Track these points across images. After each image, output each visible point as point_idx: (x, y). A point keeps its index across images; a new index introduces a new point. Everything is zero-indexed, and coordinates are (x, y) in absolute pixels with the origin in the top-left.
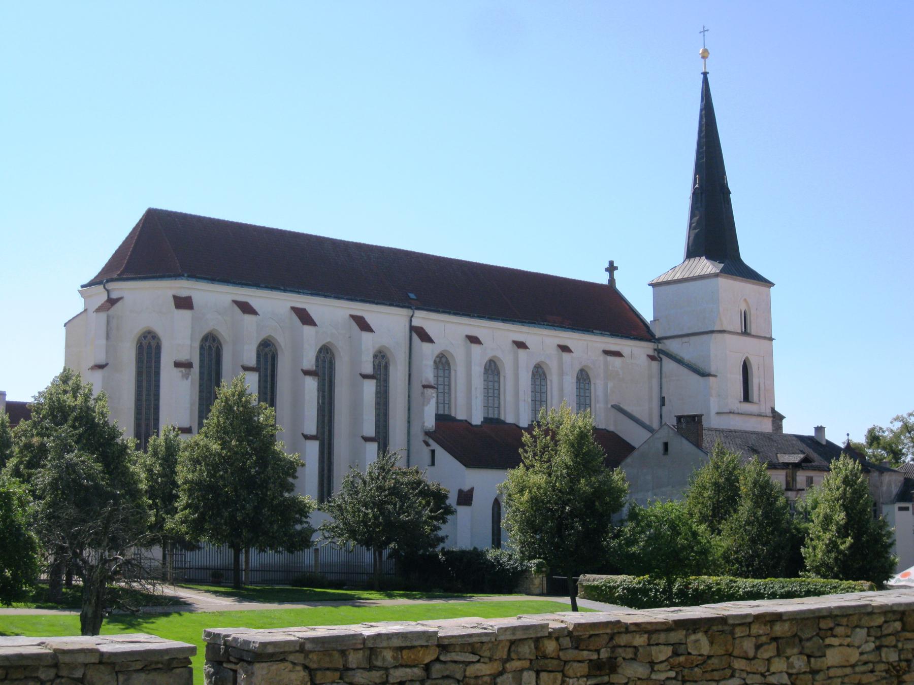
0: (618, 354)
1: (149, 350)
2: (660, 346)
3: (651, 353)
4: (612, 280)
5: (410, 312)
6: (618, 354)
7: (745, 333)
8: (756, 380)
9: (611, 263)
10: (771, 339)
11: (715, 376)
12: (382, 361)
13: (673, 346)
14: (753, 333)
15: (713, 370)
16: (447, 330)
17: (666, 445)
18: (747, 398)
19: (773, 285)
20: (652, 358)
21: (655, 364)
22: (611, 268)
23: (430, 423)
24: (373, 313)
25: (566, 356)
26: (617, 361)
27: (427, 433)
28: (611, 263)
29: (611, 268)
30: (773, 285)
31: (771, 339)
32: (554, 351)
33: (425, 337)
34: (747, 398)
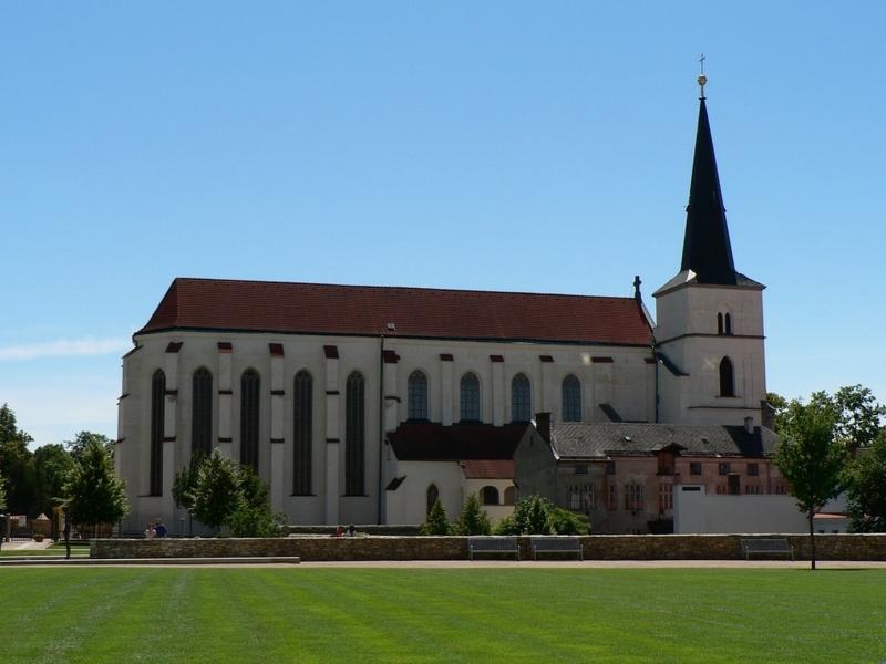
0: (609, 360)
1: (159, 380)
2: (658, 350)
3: (650, 356)
4: (638, 293)
5: (379, 340)
6: (609, 360)
7: (729, 334)
8: (738, 378)
9: (637, 278)
10: (763, 338)
11: (688, 375)
12: (355, 384)
13: (667, 350)
14: (735, 333)
15: (685, 368)
16: (418, 353)
17: (532, 438)
18: (727, 388)
19: (765, 287)
20: (648, 361)
21: (651, 367)
22: (637, 283)
23: (391, 425)
24: (345, 345)
25: (547, 365)
26: (606, 366)
27: (389, 435)
28: (637, 278)
29: (637, 283)
30: (765, 287)
31: (763, 338)
32: (537, 361)
33: (389, 357)
34: (727, 388)
